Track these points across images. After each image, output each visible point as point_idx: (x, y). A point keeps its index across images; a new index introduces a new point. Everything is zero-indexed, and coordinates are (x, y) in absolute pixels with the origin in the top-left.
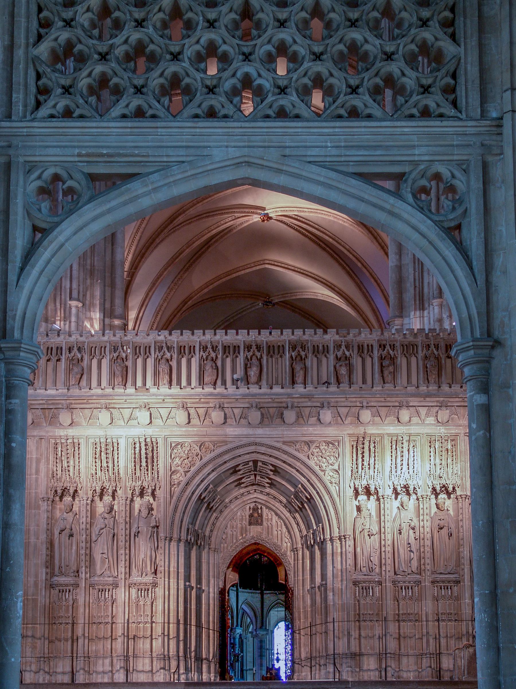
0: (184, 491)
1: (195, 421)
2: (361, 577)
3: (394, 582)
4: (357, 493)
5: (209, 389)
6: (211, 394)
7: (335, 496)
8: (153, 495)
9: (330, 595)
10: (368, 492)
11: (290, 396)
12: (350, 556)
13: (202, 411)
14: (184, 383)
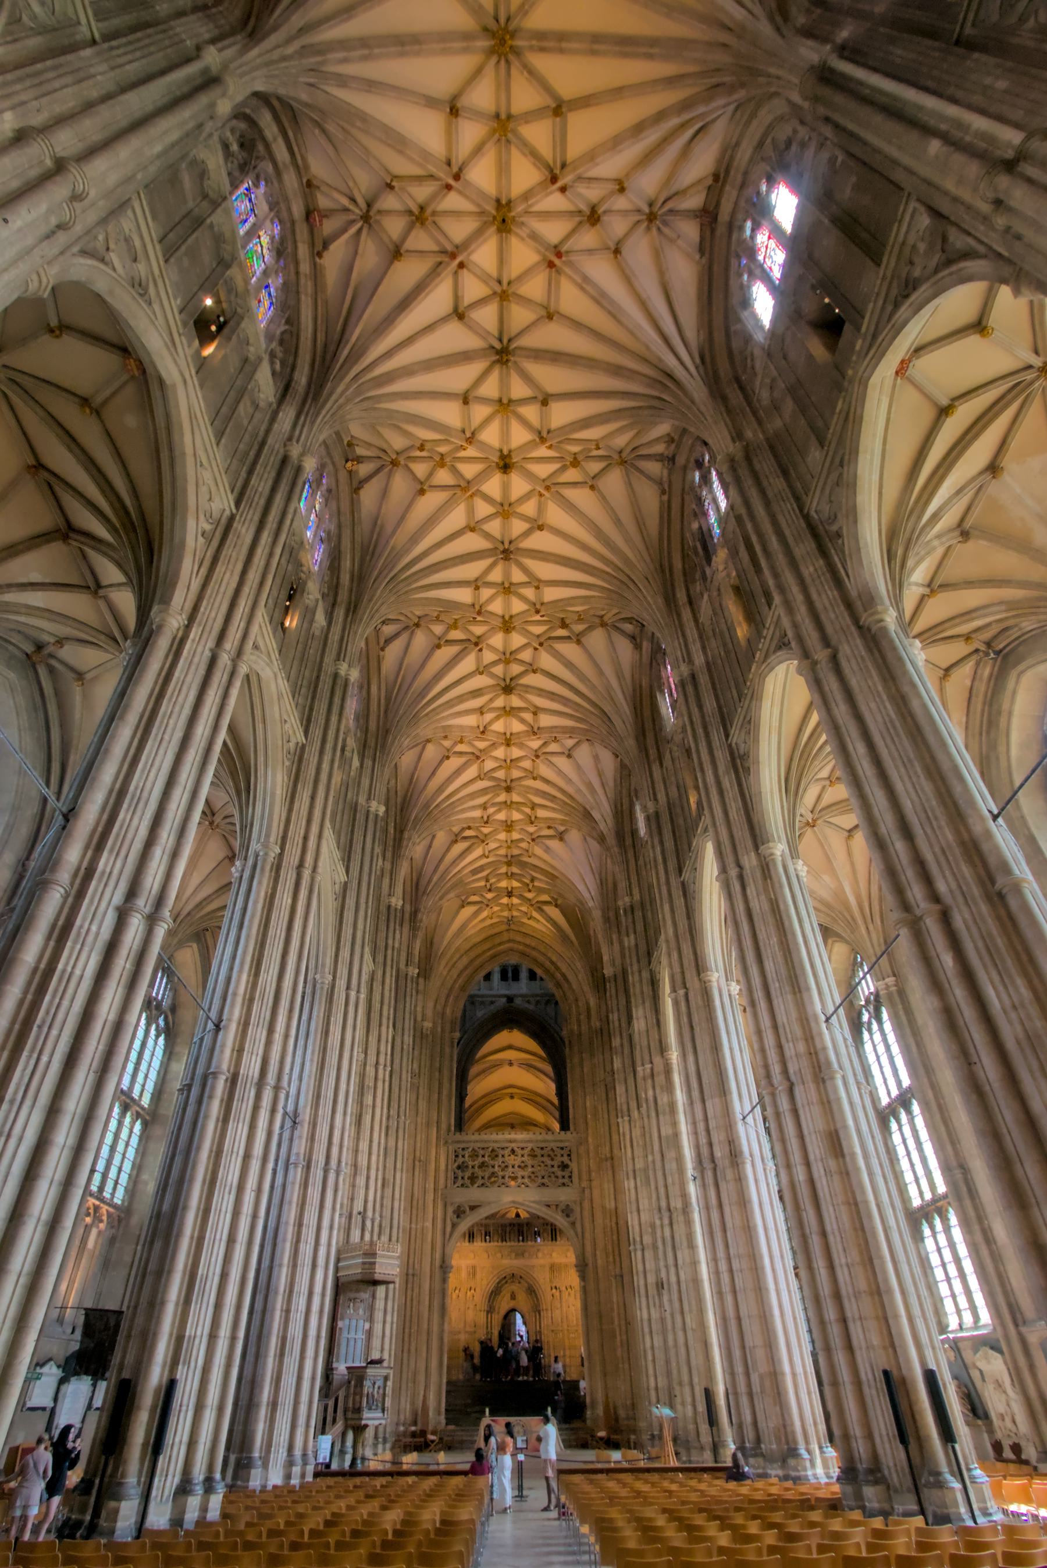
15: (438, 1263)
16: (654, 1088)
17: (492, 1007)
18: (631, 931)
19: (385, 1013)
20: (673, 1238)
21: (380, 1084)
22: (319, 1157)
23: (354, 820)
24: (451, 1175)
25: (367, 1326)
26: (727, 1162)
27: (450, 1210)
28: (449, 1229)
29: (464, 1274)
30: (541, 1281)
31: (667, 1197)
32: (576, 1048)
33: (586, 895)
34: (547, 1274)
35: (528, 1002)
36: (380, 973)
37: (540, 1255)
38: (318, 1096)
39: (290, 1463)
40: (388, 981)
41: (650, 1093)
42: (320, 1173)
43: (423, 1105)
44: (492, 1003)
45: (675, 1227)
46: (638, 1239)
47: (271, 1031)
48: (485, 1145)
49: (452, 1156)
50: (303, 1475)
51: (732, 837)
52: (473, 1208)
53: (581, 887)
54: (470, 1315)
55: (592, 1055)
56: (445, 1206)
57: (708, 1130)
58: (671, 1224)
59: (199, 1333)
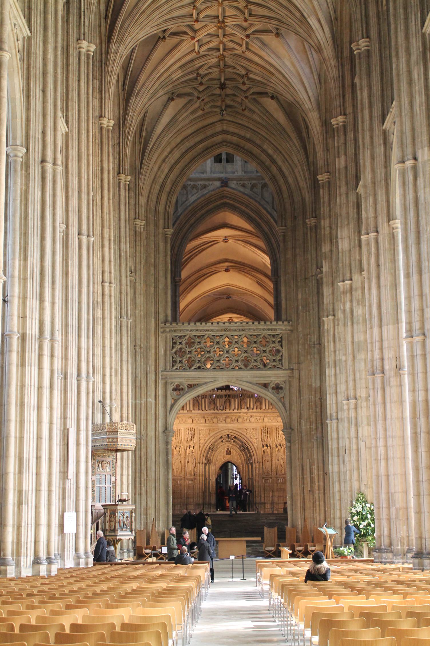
0: (204, 446)
1: (207, 422)
2: (265, 476)
3: (276, 478)
4: (263, 446)
5: (212, 411)
6: (213, 413)
7: (256, 447)
8: (194, 448)
9: (255, 482)
10: (267, 446)
11: (240, 413)
12: (261, 469)
13: (209, 418)
14: (203, 408)
15: (161, 430)
16: (351, 301)
17: (205, 191)
18: (342, 152)
19: (106, 235)
20: (356, 418)
21: (107, 299)
22: (73, 371)
23: (68, 65)
24: (169, 359)
25: (113, 479)
26: (392, 373)
27: (170, 388)
28: (169, 403)
29: (183, 436)
30: (254, 441)
31: (355, 389)
32: (289, 245)
33: (303, 95)
34: (260, 436)
35: (243, 186)
36: (98, 198)
37: (252, 420)
38: (66, 326)
39: (78, 557)
40: (106, 204)
41: (348, 305)
42: (75, 382)
43: (140, 299)
44: (205, 187)
45: (359, 410)
46: (334, 414)
47: (42, 300)
48: (201, 334)
49: (170, 344)
50: (87, 564)
51: (413, 129)
52: (191, 387)
53: (298, 87)
54: (190, 467)
55: (305, 251)
56: (166, 383)
57: (381, 349)
58: (356, 408)
59: (30, 489)
